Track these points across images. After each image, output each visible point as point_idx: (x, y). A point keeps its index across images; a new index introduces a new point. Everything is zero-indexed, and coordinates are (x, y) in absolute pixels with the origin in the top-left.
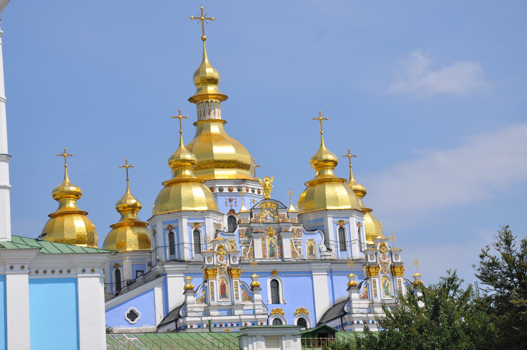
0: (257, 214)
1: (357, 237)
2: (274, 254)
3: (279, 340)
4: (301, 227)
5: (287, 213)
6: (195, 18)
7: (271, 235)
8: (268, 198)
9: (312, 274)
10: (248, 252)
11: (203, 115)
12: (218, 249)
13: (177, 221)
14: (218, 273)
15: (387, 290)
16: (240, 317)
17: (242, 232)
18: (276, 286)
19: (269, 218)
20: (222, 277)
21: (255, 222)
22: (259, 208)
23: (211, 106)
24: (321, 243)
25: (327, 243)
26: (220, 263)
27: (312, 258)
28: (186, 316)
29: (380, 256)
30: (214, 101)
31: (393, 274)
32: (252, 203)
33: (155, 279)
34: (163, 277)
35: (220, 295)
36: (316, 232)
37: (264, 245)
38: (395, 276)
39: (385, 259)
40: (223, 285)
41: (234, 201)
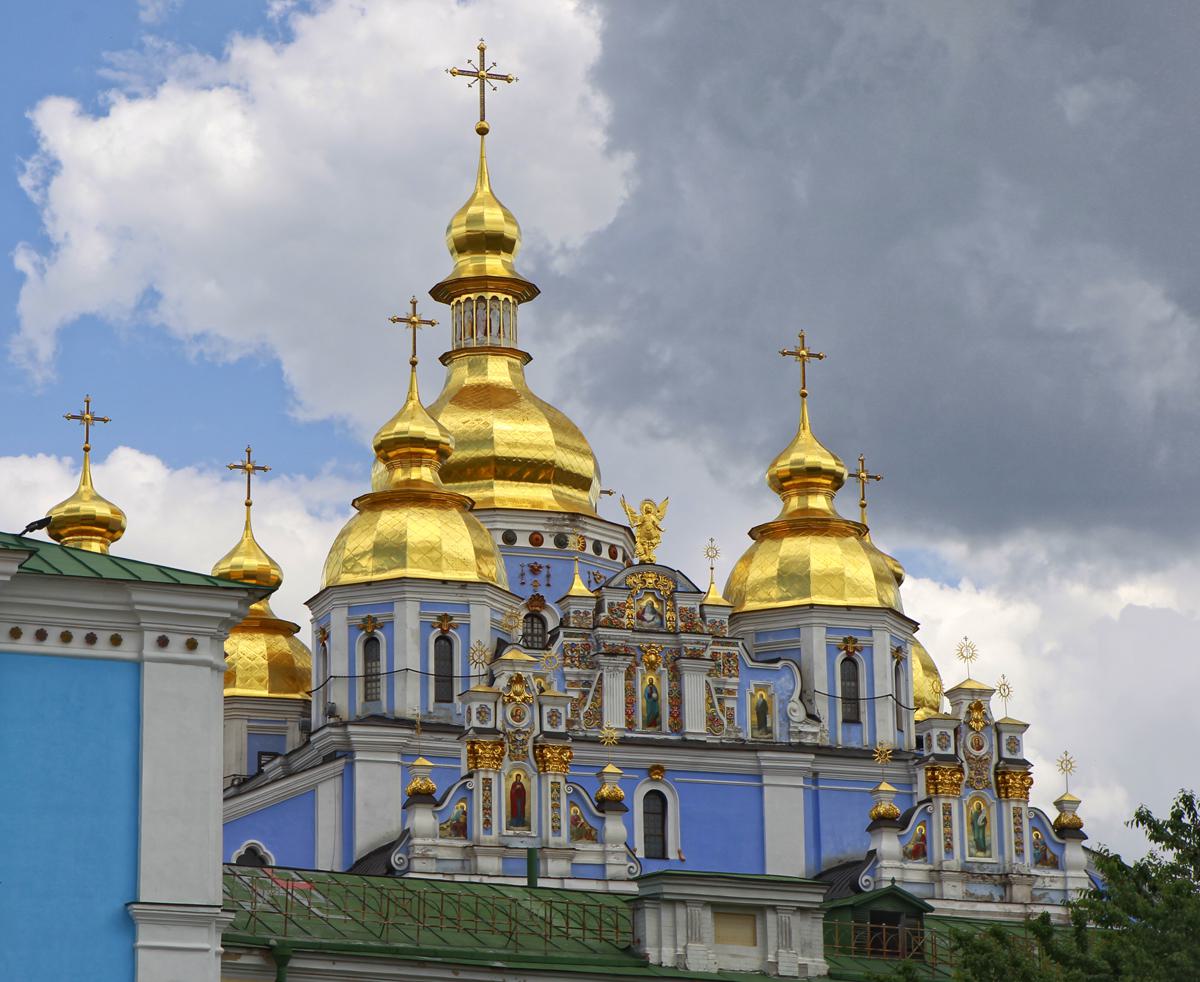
0: (615, 602)
1: (890, 689)
2: (658, 720)
3: (755, 921)
4: (737, 648)
5: (701, 606)
6: (462, 73)
7: (652, 666)
8: (650, 560)
9: (761, 781)
10: (586, 708)
11: (467, 336)
12: (509, 687)
13: (390, 605)
14: (507, 753)
15: (981, 837)
16: (563, 884)
17: (572, 652)
18: (659, 810)
19: (648, 616)
20: (515, 765)
21: (608, 624)
22: (624, 586)
23: (491, 310)
24: (790, 696)
25: (810, 698)
26: (512, 726)
27: (764, 737)
28: (408, 870)
29: (969, 738)
30: (502, 297)
31: (1002, 789)
32: (593, 582)
33: (321, 764)
34: (343, 761)
35: (509, 819)
36: (779, 665)
37: (630, 693)
38: (1007, 797)
39: (980, 748)
40: (519, 789)
41: (544, 572)
